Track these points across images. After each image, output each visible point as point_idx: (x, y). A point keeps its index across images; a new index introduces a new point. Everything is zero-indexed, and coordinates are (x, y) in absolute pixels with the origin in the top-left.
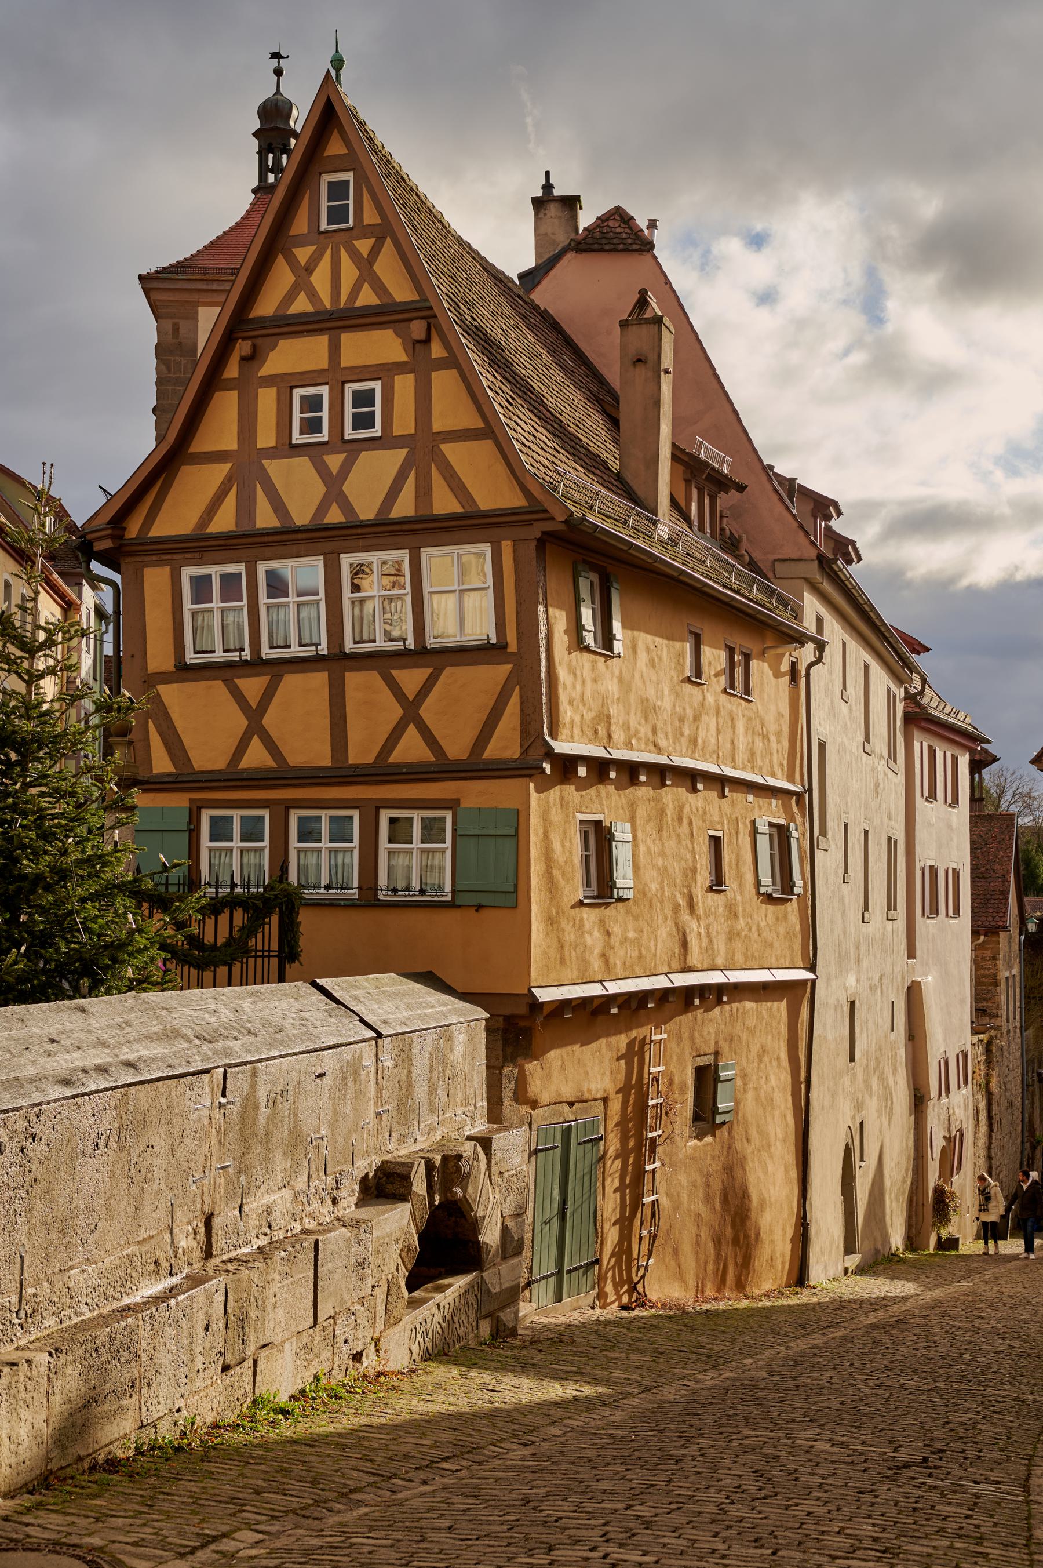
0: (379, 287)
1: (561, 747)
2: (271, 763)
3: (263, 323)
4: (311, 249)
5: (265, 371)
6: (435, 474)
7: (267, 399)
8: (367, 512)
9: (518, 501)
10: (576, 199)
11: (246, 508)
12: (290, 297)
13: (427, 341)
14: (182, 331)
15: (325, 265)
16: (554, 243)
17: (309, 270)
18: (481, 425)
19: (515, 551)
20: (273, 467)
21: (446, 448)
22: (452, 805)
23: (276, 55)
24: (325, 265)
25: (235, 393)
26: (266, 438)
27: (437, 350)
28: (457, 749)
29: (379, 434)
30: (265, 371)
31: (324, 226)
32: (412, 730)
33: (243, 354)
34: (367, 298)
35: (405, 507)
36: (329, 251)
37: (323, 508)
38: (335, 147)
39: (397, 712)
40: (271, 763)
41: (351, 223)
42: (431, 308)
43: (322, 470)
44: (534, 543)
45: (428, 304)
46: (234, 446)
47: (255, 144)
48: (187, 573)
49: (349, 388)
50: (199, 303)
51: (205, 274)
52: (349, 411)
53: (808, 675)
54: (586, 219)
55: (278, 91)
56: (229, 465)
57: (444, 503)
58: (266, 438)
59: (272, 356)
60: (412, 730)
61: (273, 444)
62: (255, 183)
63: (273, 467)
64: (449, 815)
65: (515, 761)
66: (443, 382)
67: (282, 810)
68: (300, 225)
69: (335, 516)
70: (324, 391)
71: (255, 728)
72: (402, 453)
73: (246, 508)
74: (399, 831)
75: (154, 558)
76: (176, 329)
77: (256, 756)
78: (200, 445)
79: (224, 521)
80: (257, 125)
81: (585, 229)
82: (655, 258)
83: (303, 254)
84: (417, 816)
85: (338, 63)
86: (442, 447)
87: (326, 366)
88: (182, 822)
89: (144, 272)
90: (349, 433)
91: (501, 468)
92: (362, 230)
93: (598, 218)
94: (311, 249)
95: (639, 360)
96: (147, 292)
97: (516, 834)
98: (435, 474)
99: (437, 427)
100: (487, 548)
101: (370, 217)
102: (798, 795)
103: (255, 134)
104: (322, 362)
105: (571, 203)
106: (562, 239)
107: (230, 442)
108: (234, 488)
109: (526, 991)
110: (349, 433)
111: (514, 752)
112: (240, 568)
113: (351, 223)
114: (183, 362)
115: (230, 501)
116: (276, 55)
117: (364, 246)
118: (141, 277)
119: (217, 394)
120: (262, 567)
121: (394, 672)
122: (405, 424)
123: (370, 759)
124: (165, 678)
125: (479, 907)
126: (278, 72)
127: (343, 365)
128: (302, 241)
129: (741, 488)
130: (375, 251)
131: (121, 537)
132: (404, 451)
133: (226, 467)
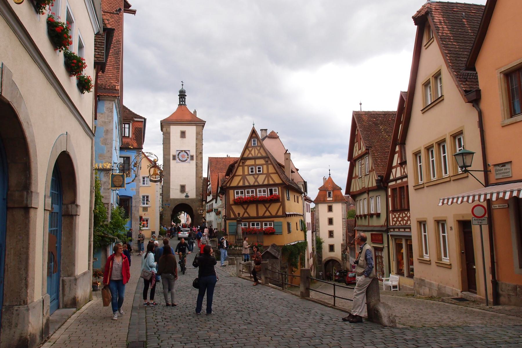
0: (261, 153)
1: (287, 213)
2: (248, 216)
5: (246, 164)
6: (270, 178)
7: (246, 168)
8: (261, 183)
10: (267, 130)
11: (244, 182)
13: (267, 161)
16: (264, 136)
20: (247, 177)
22: (273, 221)
27: (269, 162)
28: (274, 214)
30: (246, 164)
31: (252, 145)
32: (267, 212)
34: (259, 155)
35: (266, 183)
37: (255, 183)
38: (254, 135)
39: (265, 209)
40: (248, 216)
41: (256, 145)
50: (171, 125)
52: (257, 170)
54: (269, 132)
55: (182, 88)
57: (271, 182)
58: (246, 173)
61: (247, 174)
62: (179, 104)
63: (247, 177)
66: (270, 167)
67: (249, 222)
68: (249, 145)
69: (256, 184)
71: (246, 211)
72: (264, 176)
73: (244, 182)
76: (167, 130)
77: (246, 215)
79: (241, 184)
83: (250, 149)
85: (254, 125)
90: (257, 172)
92: (258, 146)
96: (161, 123)
97: (282, 225)
98: (270, 179)
99: (270, 172)
101: (259, 144)
102: (302, 215)
103: (179, 95)
105: (266, 130)
106: (265, 135)
107: (241, 174)
113: (256, 145)
116: (182, 82)
118: (161, 121)
119: (239, 167)
122: (265, 172)
125: (277, 235)
126: (182, 85)
128: (250, 147)
129: (294, 172)
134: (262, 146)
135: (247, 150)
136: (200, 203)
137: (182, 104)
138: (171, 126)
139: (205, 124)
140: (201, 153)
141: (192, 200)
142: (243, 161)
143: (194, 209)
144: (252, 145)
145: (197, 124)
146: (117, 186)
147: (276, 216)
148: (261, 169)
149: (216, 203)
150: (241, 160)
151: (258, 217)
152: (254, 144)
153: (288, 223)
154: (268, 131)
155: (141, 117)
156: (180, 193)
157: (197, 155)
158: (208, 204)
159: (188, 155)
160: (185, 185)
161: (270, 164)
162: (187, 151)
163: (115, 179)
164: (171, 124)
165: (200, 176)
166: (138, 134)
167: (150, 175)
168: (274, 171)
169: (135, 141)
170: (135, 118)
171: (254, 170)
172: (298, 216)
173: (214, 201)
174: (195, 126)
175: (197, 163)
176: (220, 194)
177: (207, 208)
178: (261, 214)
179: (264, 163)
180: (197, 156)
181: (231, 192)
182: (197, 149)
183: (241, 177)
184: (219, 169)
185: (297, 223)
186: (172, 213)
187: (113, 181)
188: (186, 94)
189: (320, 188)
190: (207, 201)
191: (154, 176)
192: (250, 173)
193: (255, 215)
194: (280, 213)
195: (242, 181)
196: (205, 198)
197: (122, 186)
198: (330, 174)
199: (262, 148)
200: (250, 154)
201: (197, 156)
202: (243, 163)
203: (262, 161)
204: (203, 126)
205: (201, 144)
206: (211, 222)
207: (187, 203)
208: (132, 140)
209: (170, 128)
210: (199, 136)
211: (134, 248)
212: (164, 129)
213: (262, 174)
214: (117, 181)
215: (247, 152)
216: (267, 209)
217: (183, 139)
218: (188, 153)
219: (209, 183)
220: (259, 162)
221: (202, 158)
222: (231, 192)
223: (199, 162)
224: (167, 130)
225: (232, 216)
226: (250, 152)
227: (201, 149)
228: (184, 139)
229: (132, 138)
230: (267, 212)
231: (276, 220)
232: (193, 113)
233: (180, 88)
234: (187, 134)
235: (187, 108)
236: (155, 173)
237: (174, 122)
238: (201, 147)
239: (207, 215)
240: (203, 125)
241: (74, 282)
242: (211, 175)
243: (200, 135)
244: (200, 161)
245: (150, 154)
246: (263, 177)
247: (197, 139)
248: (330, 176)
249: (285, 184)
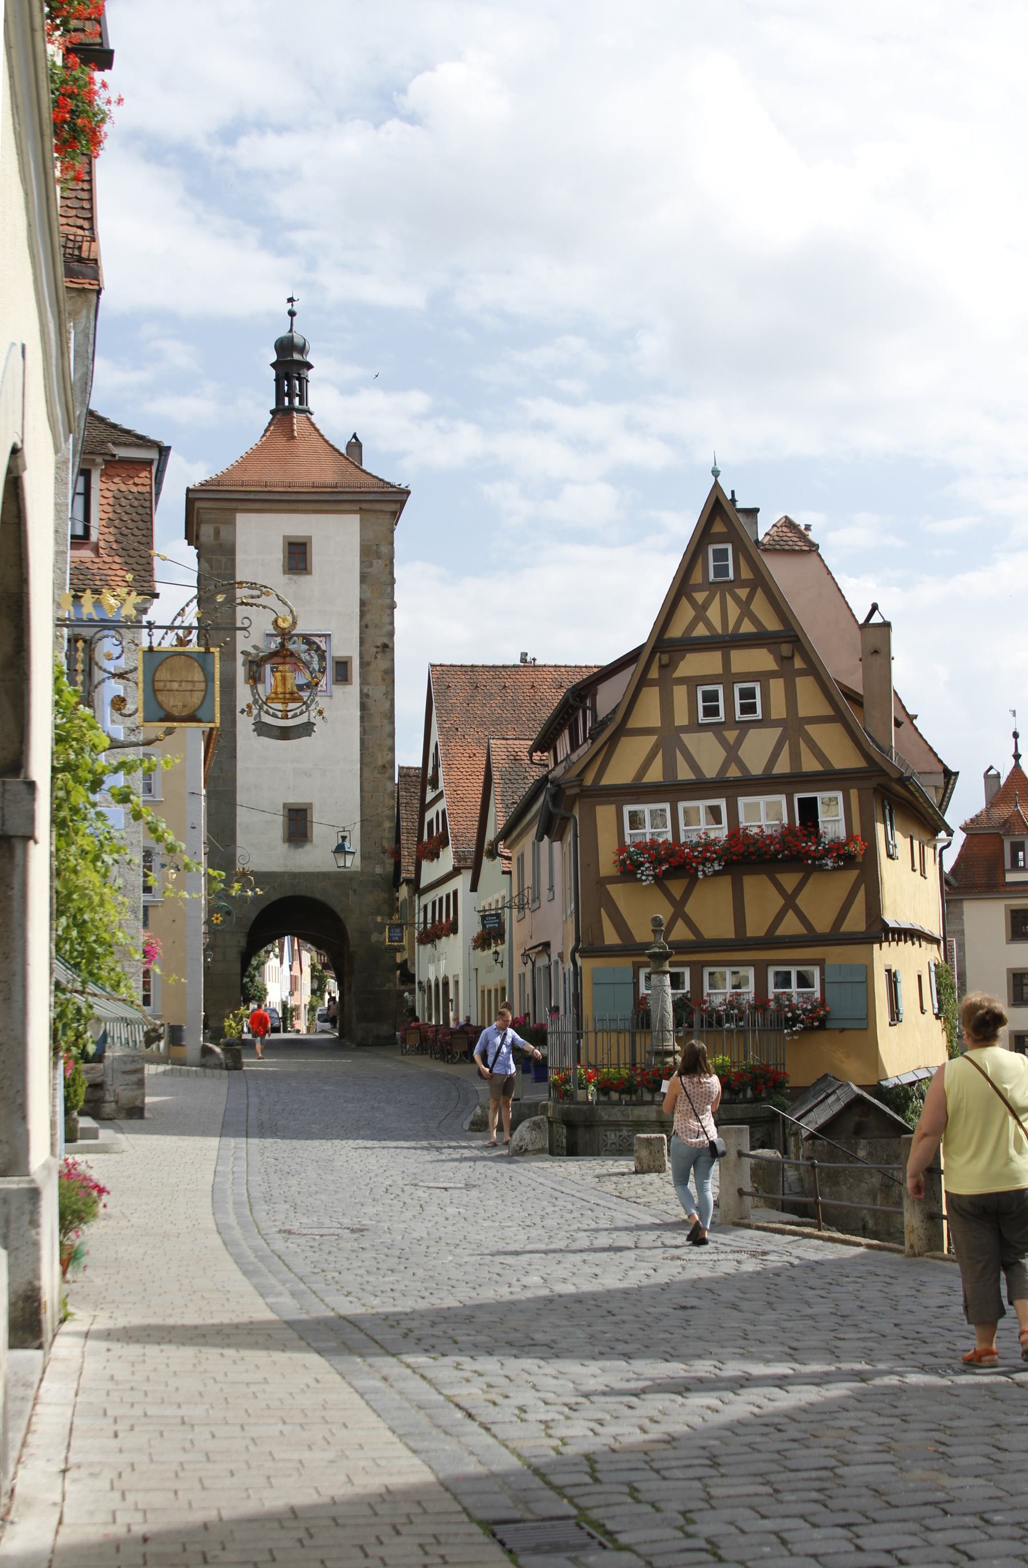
0: (755, 620)
3: (673, 642)
4: (705, 594)
5: (677, 674)
7: (680, 693)
8: (756, 768)
9: (860, 763)
10: (757, 510)
11: (670, 766)
12: (692, 625)
13: (792, 658)
14: (223, 533)
15: (716, 604)
17: (705, 606)
18: (832, 713)
19: (859, 796)
20: (685, 738)
21: (809, 728)
22: (820, 963)
23: (291, 300)
24: (716, 604)
25: (657, 689)
26: (681, 719)
27: (798, 663)
28: (822, 925)
29: (760, 717)
30: (677, 674)
31: (711, 578)
32: (790, 914)
33: (663, 662)
34: (747, 627)
35: (783, 766)
36: (718, 595)
38: (718, 527)
39: (781, 902)
40: (691, 937)
42: (797, 636)
43: (723, 742)
44: (872, 791)
45: (792, 633)
46: (659, 724)
47: (272, 373)
48: (627, 809)
49: (737, 688)
51: (242, 486)
53: (941, 856)
56: (655, 737)
57: (810, 764)
58: (681, 719)
59: (682, 664)
60: (790, 913)
61: (686, 723)
62: (273, 406)
63: (685, 738)
64: (816, 971)
65: (862, 933)
66: (805, 685)
68: (697, 578)
69: (733, 772)
70: (720, 689)
71: (679, 912)
72: (778, 731)
73: (670, 766)
74: (784, 980)
75: (604, 799)
76: (217, 533)
78: (633, 723)
79: (655, 774)
80: (273, 357)
81: (767, 534)
82: (820, 556)
83: (700, 597)
84: (794, 971)
85: (716, 473)
86: (806, 727)
87: (721, 672)
88: (629, 978)
89: (191, 487)
91: (849, 743)
92: (738, 582)
93: (774, 526)
94: (705, 594)
95: (876, 652)
96: (190, 502)
97: (865, 982)
99: (802, 713)
100: (839, 795)
101: (746, 574)
103: (272, 365)
104: (719, 670)
108: (660, 753)
109: (875, 1083)
110: (738, 716)
111: (861, 927)
112: (667, 806)
113: (731, 576)
114: (224, 560)
115: (658, 762)
117: (743, 593)
118: (189, 491)
120: (682, 806)
121: (778, 876)
122: (778, 711)
123: (762, 933)
124: (612, 880)
125: (842, 1030)
126: (292, 314)
127: (733, 671)
128: (699, 588)
130: (751, 597)
131: (580, 786)
132: (780, 729)
133: (654, 738)
134: (761, 582)
135: (684, 601)
136: (386, 896)
137: (291, 409)
138: (241, 519)
139: (402, 503)
140: (387, 649)
141: (342, 880)
142: (665, 659)
143: (352, 923)
144: (711, 578)
145: (365, 506)
146: (176, 713)
147: (836, 938)
148: (758, 700)
149: (474, 888)
150: (653, 653)
151: (741, 943)
152: (722, 571)
153: (888, 971)
154: (759, 515)
155: (143, 442)
156: (286, 845)
157: (367, 659)
158: (427, 899)
159: (322, 657)
160: (311, 804)
161: (801, 673)
162: (317, 640)
163: (163, 674)
164: (241, 506)
165: (380, 763)
166: (131, 525)
167: (256, 702)
168: (824, 709)
169: (117, 559)
170: (114, 444)
171: (721, 703)
172: (923, 943)
173: (461, 883)
174: (356, 518)
175: (364, 696)
176: (501, 846)
177: (419, 918)
178: (756, 928)
179: (776, 668)
180: (364, 664)
181: (604, 813)
182: (364, 628)
183: (654, 738)
184: (482, 724)
185: (920, 977)
186: (243, 942)
187: (152, 690)
188: (310, 358)
189: (972, 820)
190: (423, 884)
191: (280, 707)
192: (701, 718)
193: (726, 931)
194: (856, 922)
195: (659, 757)
196: (412, 868)
197: (200, 714)
198: (1017, 756)
199: (759, 591)
200: (701, 625)
201: (368, 664)
202: (662, 667)
203: (761, 659)
204: (396, 515)
205: (388, 601)
206: (446, 984)
207: (318, 895)
208: (98, 555)
209: (232, 523)
210: (378, 564)
211: (116, 1095)
212: (206, 532)
213: (765, 722)
214: (175, 686)
215: (686, 613)
216: (790, 902)
217: (295, 577)
218: (323, 646)
219: (430, 795)
220: (746, 660)
221: (389, 674)
222: (604, 813)
223: (377, 692)
224: (217, 533)
225: (611, 937)
226: (701, 610)
227: (389, 627)
228: (304, 579)
229: (102, 544)
230: (790, 915)
231: (835, 955)
232: (343, 451)
233: (284, 333)
234: (317, 556)
235: (313, 424)
236: (280, 690)
237: (251, 496)
238: (386, 619)
239: (423, 952)
240: (393, 507)
241: (28, 1207)
242: (445, 755)
243: (379, 558)
244: (383, 688)
245: (258, 593)
246: (769, 737)
247: (364, 578)
248: (1017, 768)
249: (883, 772)
